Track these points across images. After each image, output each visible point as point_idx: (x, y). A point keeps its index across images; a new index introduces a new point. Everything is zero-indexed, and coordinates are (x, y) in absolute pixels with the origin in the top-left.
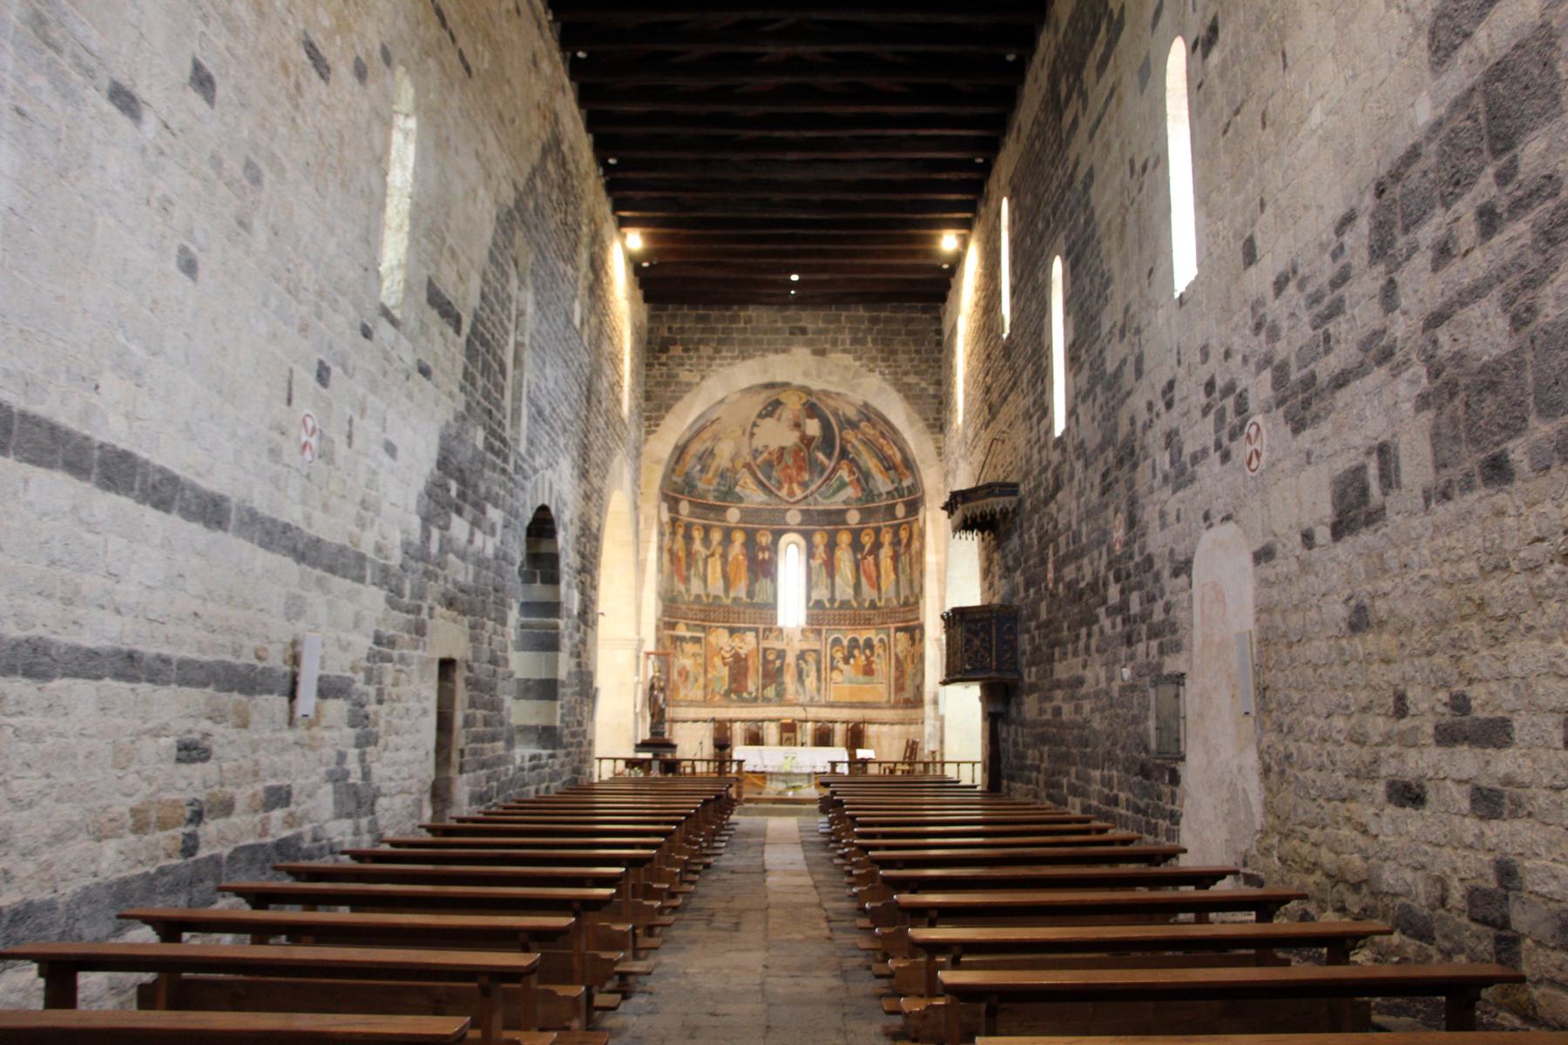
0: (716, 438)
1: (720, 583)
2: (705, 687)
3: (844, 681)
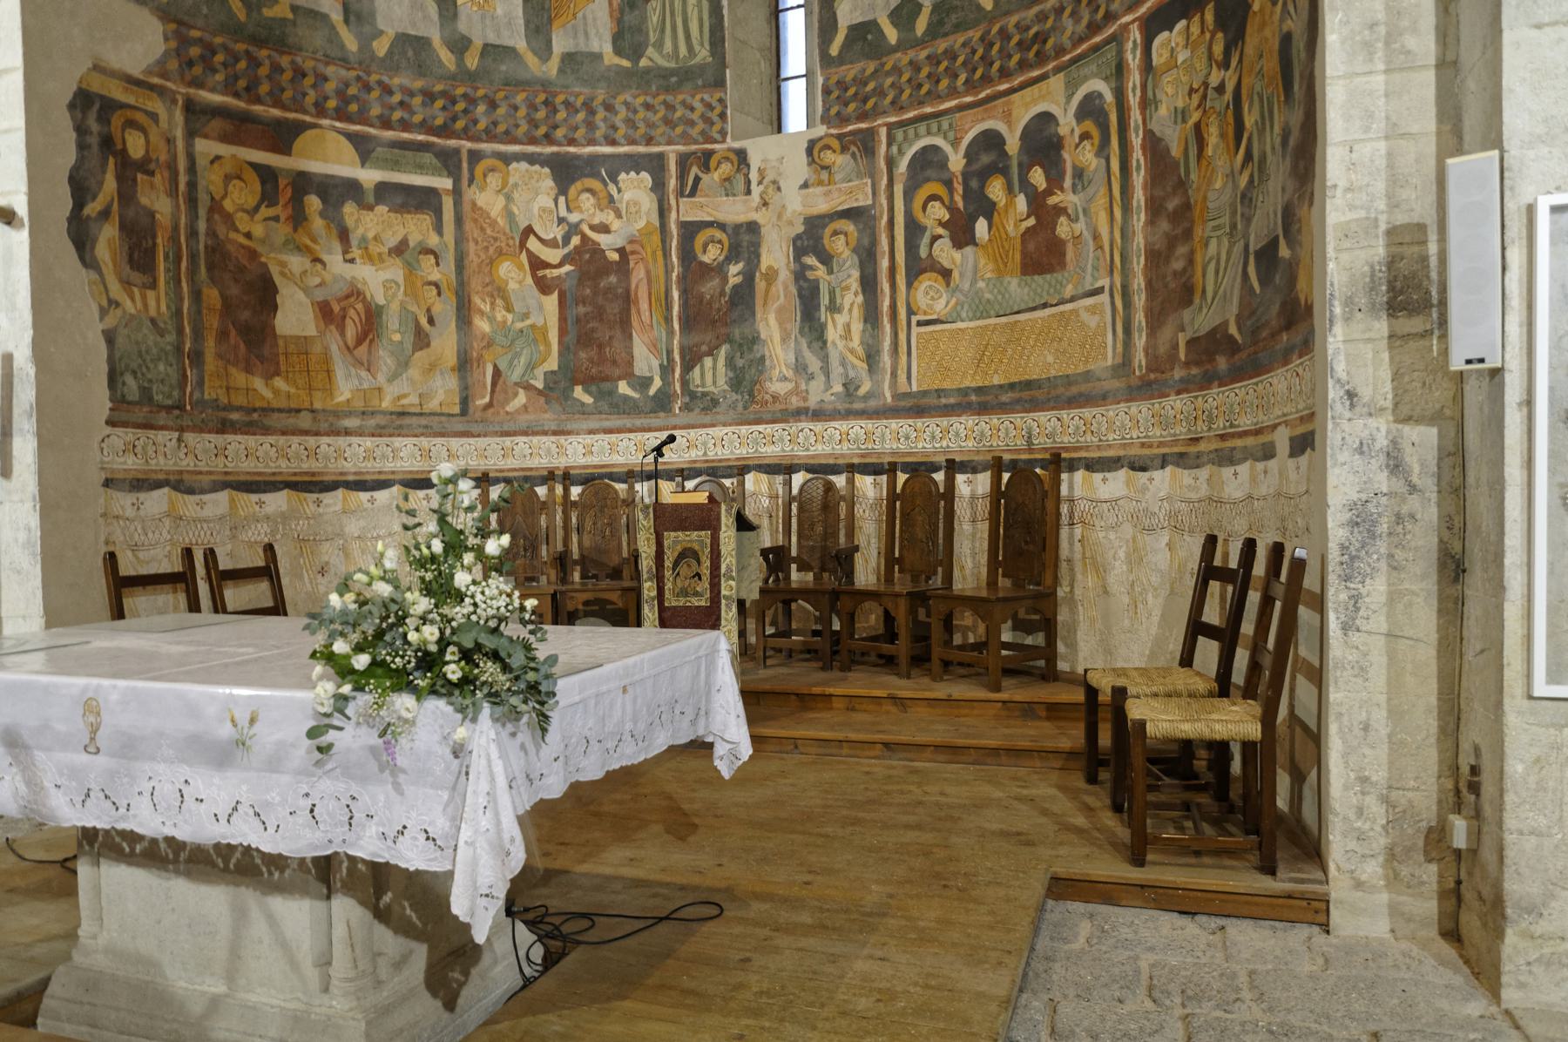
2: (464, 364)
3: (960, 315)
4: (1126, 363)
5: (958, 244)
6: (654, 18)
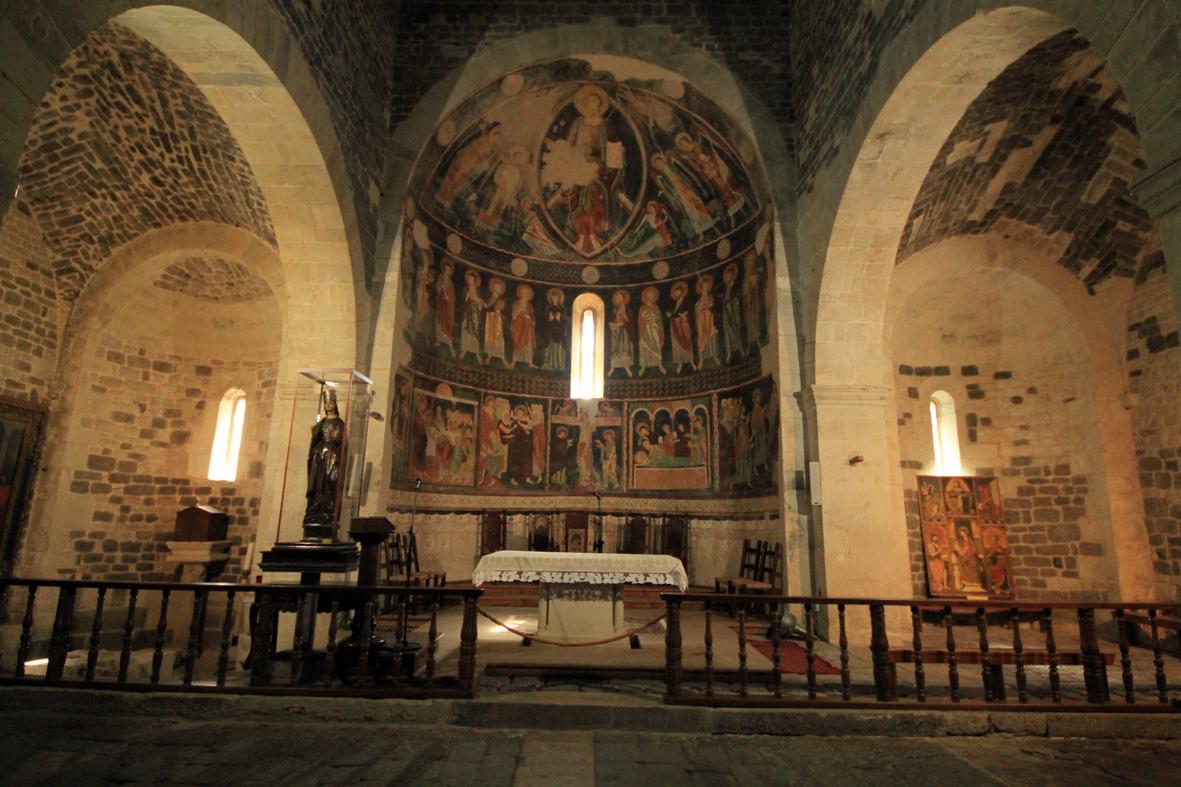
0: (496, 159)
1: (501, 344)
2: (477, 468)
3: (650, 466)
4: (712, 488)
5: (652, 443)
6: (547, 354)
